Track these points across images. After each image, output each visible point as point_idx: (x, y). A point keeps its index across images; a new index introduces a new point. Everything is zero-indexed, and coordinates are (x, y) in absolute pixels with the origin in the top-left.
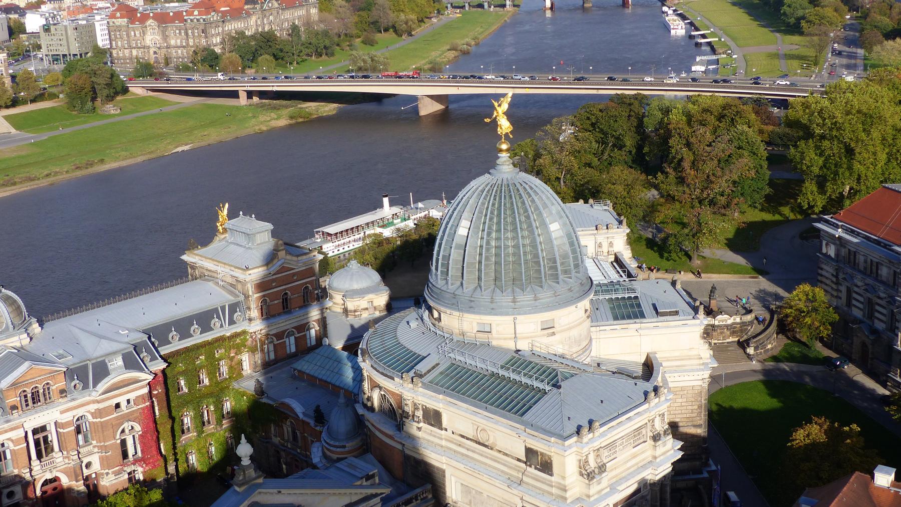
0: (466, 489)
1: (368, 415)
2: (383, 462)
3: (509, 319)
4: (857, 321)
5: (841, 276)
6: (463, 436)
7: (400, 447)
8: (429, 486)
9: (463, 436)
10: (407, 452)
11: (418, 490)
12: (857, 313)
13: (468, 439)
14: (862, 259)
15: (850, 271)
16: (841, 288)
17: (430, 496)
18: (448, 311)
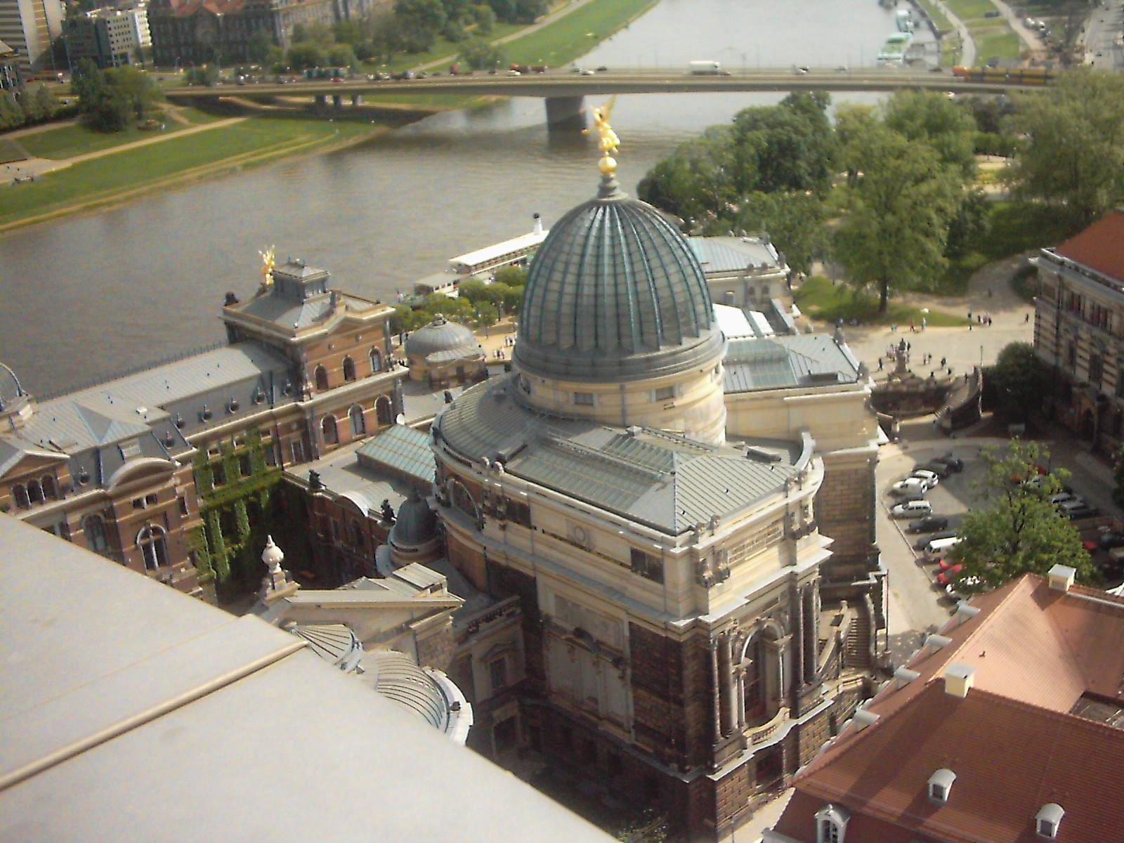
0: (561, 601)
1: (442, 513)
2: (460, 569)
3: (614, 387)
4: (1083, 385)
5: (1063, 326)
6: (555, 536)
7: (481, 550)
8: (516, 598)
9: (555, 536)
10: (490, 556)
11: (501, 604)
12: (1082, 375)
13: (561, 539)
14: (1088, 304)
15: (1072, 318)
16: (1063, 342)
17: (519, 611)
18: (540, 379)
